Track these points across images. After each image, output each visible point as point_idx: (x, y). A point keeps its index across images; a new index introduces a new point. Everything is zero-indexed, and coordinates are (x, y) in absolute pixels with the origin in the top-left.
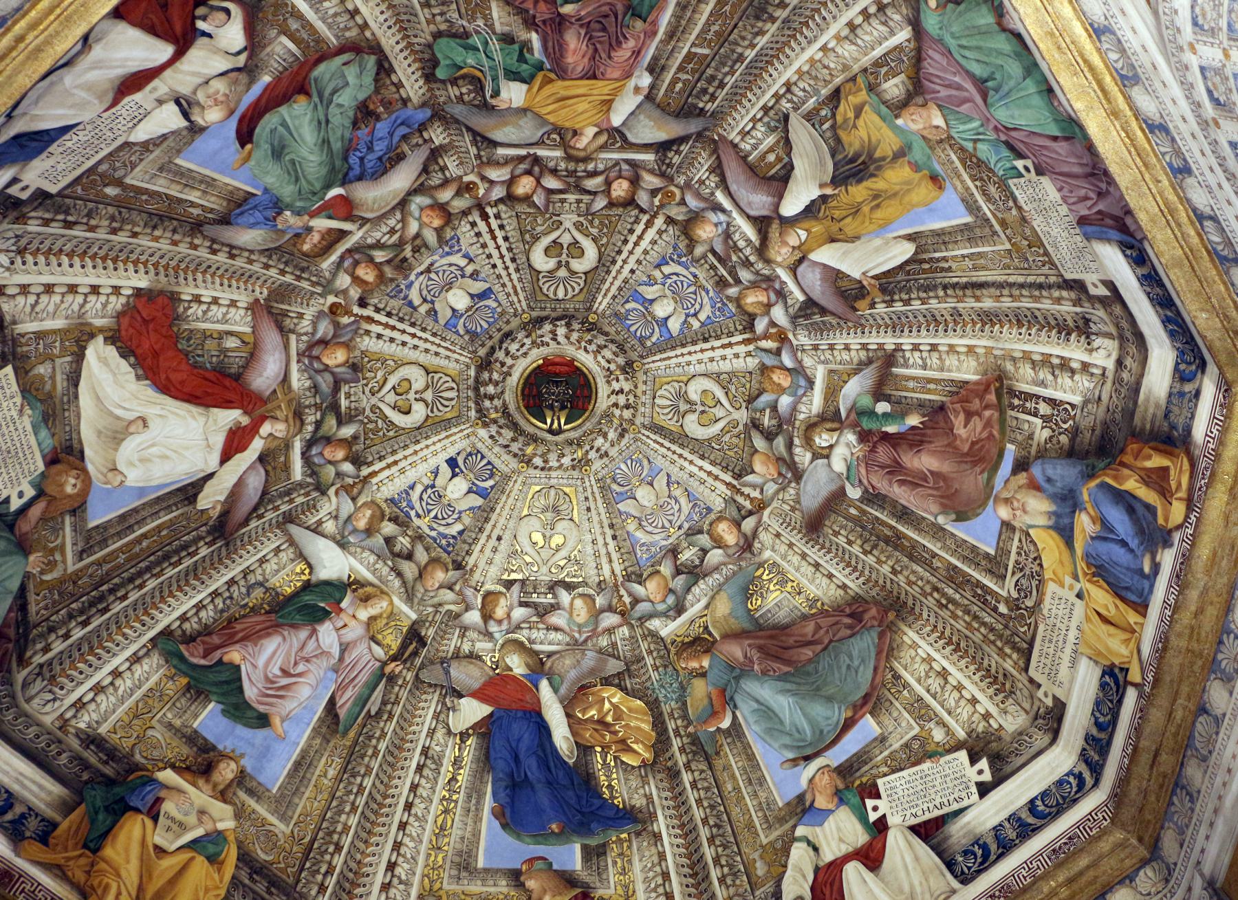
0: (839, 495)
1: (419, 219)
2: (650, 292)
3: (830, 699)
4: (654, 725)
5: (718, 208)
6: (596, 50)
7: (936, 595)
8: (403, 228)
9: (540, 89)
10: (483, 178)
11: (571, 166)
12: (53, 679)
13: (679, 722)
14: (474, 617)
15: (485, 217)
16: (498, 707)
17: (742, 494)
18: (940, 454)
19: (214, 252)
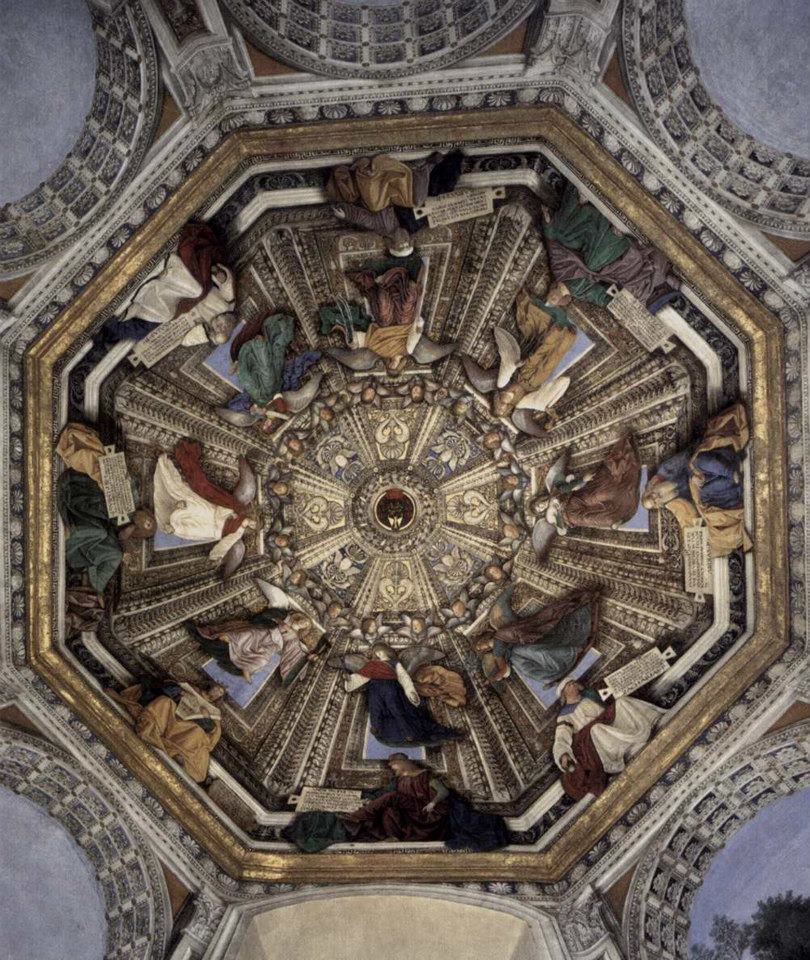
0: (554, 536)
1: (319, 415)
2: (438, 449)
3: (567, 647)
4: (465, 685)
5: (467, 394)
6: (395, 306)
7: (621, 573)
8: (312, 420)
9: (372, 334)
10: (349, 392)
11: (391, 380)
12: (129, 627)
13: (479, 680)
14: (357, 632)
15: (351, 414)
16: (372, 679)
17: (501, 551)
18: (608, 490)
19: (221, 425)
